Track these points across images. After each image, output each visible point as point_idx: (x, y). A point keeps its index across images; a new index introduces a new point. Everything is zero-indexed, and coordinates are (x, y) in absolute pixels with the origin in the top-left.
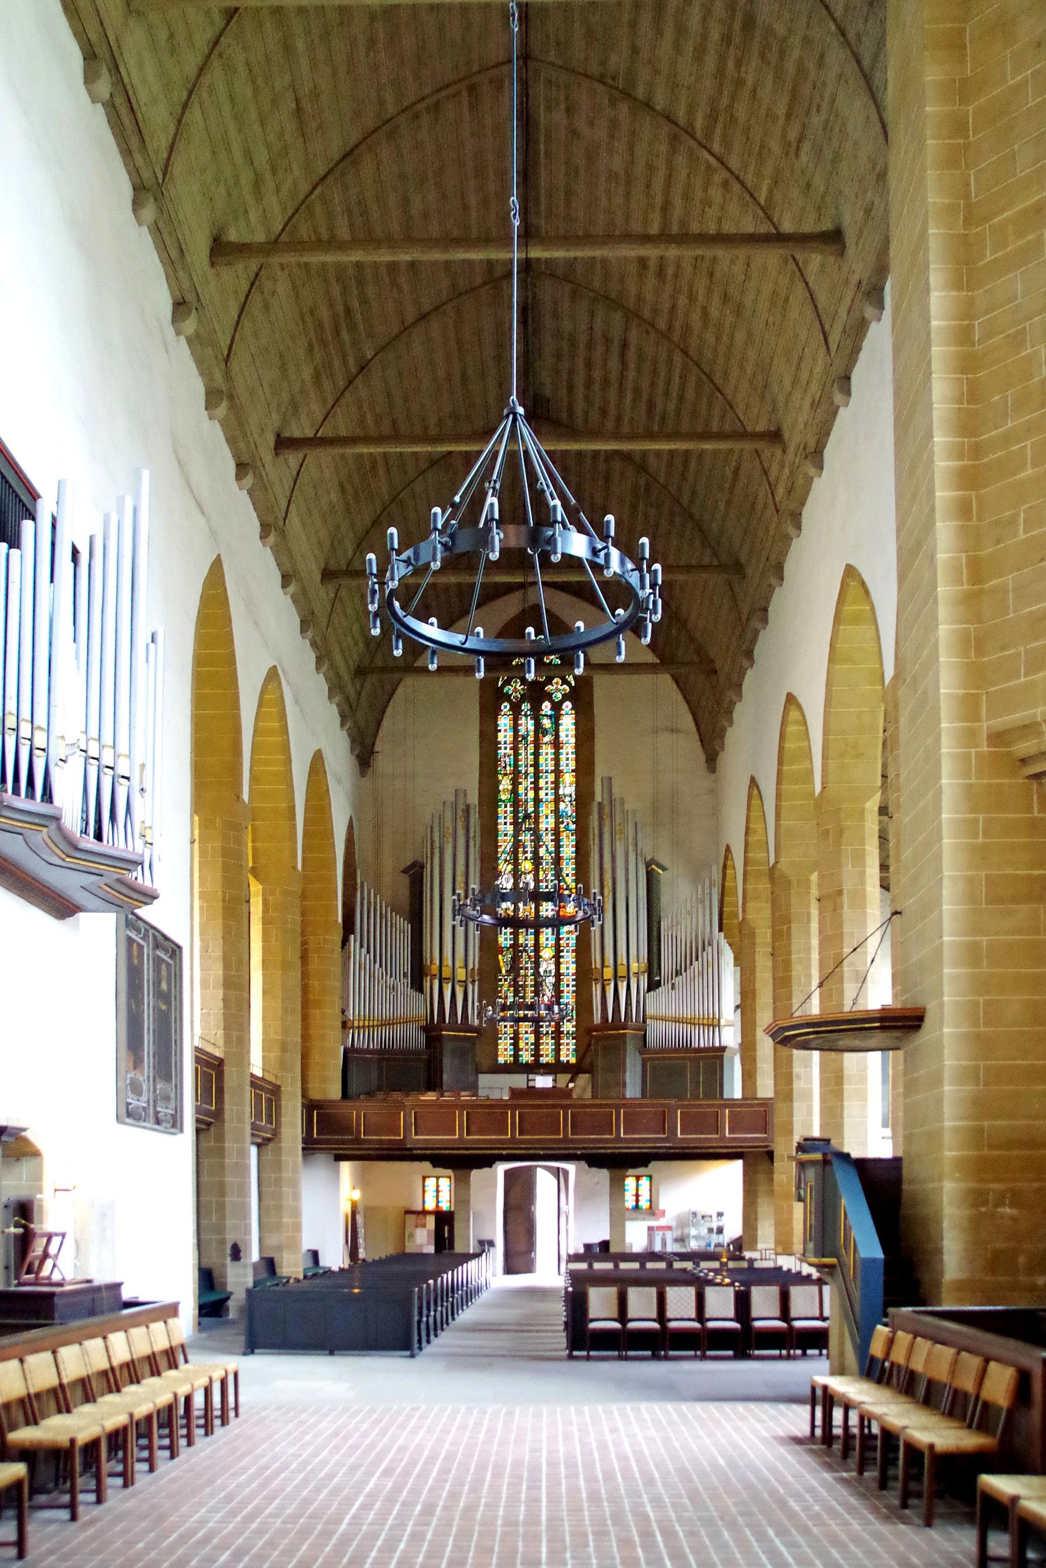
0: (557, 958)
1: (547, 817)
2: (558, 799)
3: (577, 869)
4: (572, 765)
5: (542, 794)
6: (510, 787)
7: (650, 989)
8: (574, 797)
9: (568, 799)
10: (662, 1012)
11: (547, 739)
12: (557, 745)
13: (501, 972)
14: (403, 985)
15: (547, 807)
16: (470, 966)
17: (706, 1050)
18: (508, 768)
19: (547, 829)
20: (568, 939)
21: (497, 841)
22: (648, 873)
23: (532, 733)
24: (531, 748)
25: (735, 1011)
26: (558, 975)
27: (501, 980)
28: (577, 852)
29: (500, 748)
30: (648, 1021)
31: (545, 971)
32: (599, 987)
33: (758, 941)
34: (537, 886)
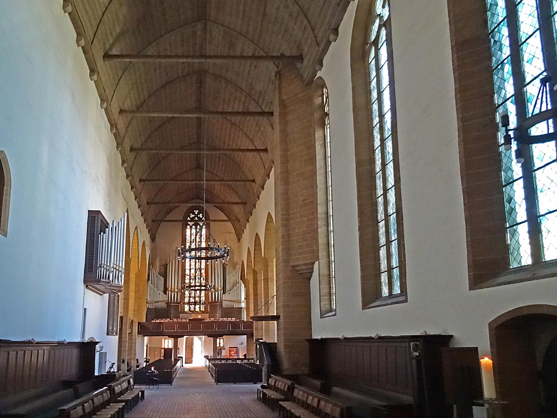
11: (198, 234)
12: (201, 236)
17: (237, 308)
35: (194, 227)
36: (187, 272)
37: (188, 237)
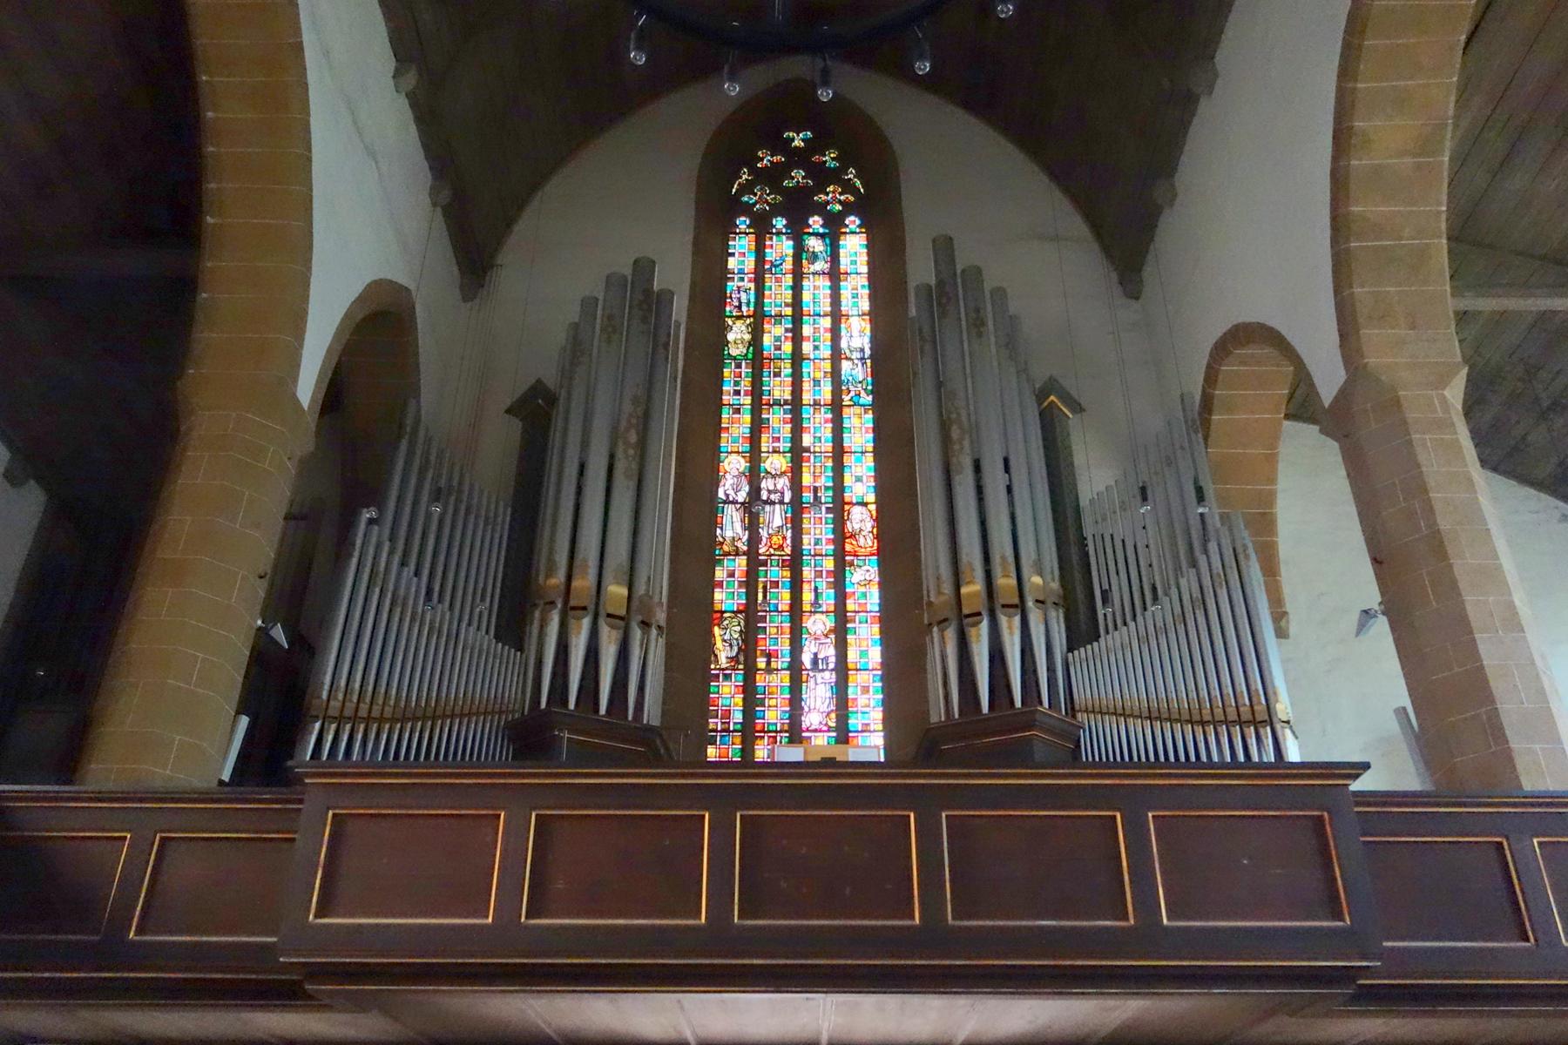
0: (840, 632)
1: (817, 382)
2: (837, 356)
4: (865, 305)
5: (807, 347)
6: (747, 337)
7: (1070, 649)
8: (868, 352)
9: (856, 355)
10: (1109, 694)
11: (820, 265)
14: (479, 637)
18: (744, 308)
23: (789, 260)
24: (788, 280)
25: (1362, 627)
32: (951, 635)
33: (1412, 415)
34: (786, 731)
35: (780, 223)
36: (732, 526)
37: (740, 289)
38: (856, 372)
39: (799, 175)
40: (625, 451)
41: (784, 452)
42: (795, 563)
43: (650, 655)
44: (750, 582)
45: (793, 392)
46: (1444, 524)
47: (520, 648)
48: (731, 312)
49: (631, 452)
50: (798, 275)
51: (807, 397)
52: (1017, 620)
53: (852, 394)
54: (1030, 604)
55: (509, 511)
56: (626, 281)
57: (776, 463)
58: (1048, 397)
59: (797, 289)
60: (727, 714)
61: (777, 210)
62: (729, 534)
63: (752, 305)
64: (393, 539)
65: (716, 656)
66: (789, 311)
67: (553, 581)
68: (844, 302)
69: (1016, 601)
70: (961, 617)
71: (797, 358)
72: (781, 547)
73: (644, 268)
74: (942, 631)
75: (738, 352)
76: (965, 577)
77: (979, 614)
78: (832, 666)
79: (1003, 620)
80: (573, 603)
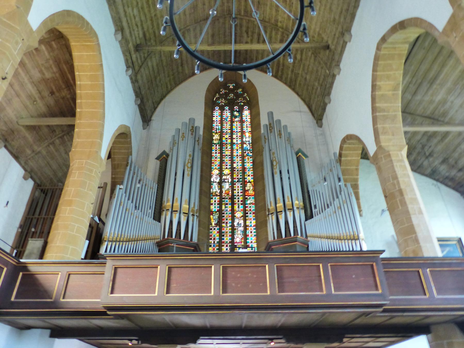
0: (245, 217)
1: (237, 150)
2: (243, 143)
3: (254, 173)
4: (249, 129)
7: (306, 220)
8: (251, 142)
9: (247, 143)
11: (237, 119)
12: (242, 122)
13: (211, 224)
15: (237, 146)
16: (192, 205)
18: (218, 131)
19: (237, 155)
20: (250, 207)
21: (211, 160)
22: (297, 158)
24: (229, 123)
26: (246, 227)
27: (211, 229)
28: (253, 165)
29: (214, 123)
30: (309, 239)
31: (238, 224)
33: (393, 158)
35: (227, 108)
36: (215, 188)
37: (216, 125)
38: (247, 146)
39: (232, 95)
40: (187, 169)
41: (229, 169)
42: (232, 198)
43: (194, 223)
44: (220, 204)
45: (231, 153)
46: (402, 187)
47: (159, 221)
48: (214, 131)
49: (189, 169)
50: (232, 122)
51: (235, 154)
52: (292, 213)
53: (247, 153)
54: (295, 208)
55: (157, 185)
56: (187, 124)
57: (227, 171)
58: (299, 154)
59: (232, 125)
60: (214, 239)
61: (226, 105)
62: (214, 191)
63: (220, 130)
64: (125, 193)
65: (211, 223)
66: (230, 131)
67: (168, 204)
68: (244, 129)
69: (291, 208)
70: (277, 212)
71: (232, 144)
72: (228, 194)
73: (192, 120)
74: (272, 216)
75: (216, 142)
76: (278, 202)
77: (281, 211)
78: (242, 225)
79: (288, 213)
80: (174, 210)
